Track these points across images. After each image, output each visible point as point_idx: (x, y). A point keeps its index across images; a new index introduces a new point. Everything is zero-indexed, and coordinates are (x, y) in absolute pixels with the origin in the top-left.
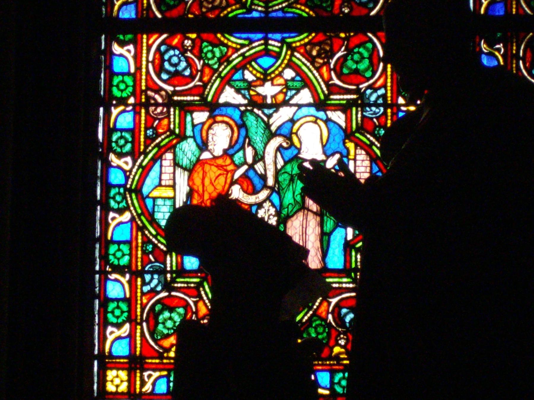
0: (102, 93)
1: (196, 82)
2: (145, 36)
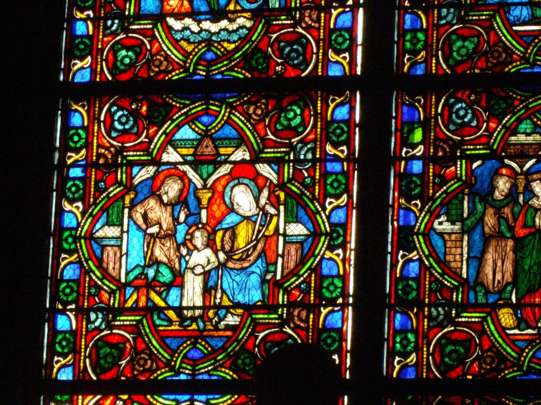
2: (80, 397)
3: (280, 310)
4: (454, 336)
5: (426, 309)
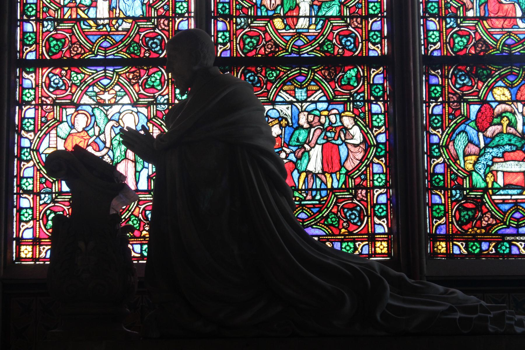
0: (18, 99)
1: (68, 93)
2: (40, 69)
3: (153, 20)
4: (250, 34)
5: (234, 19)
